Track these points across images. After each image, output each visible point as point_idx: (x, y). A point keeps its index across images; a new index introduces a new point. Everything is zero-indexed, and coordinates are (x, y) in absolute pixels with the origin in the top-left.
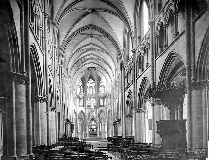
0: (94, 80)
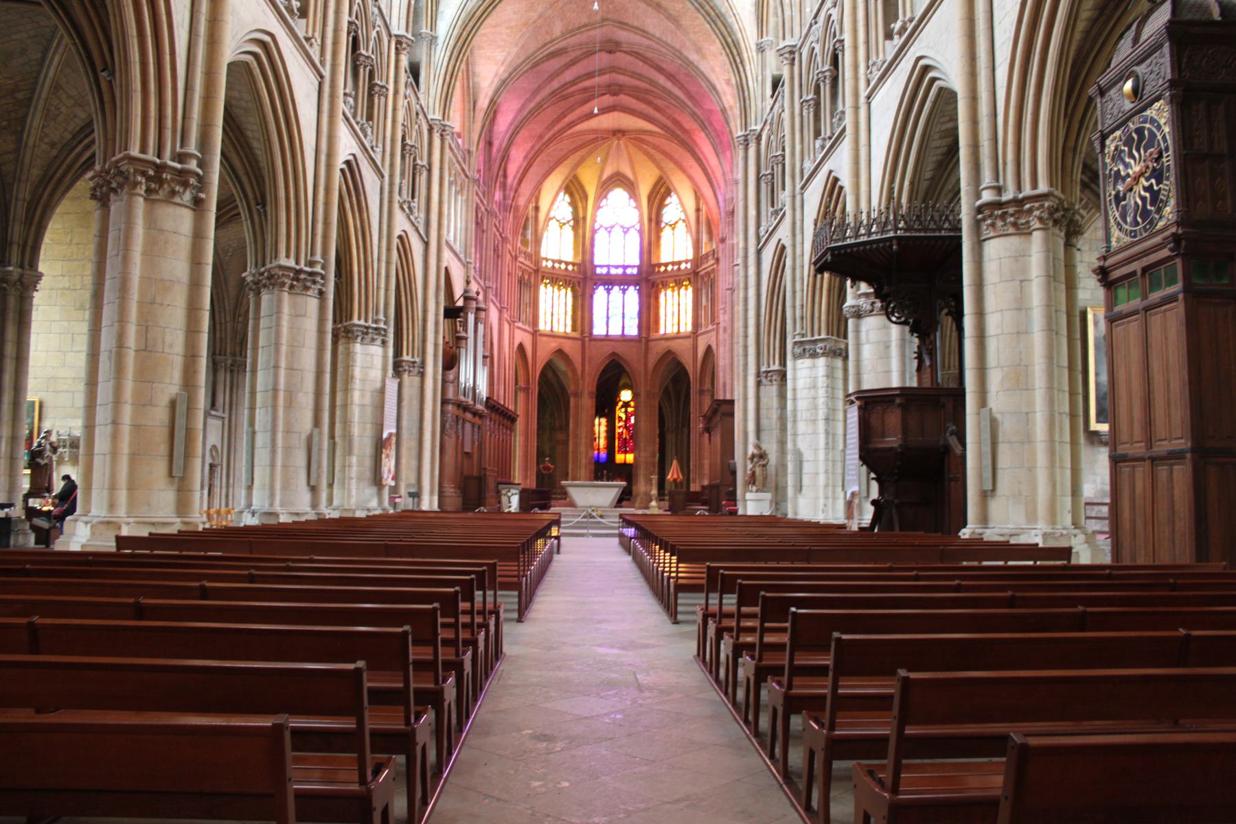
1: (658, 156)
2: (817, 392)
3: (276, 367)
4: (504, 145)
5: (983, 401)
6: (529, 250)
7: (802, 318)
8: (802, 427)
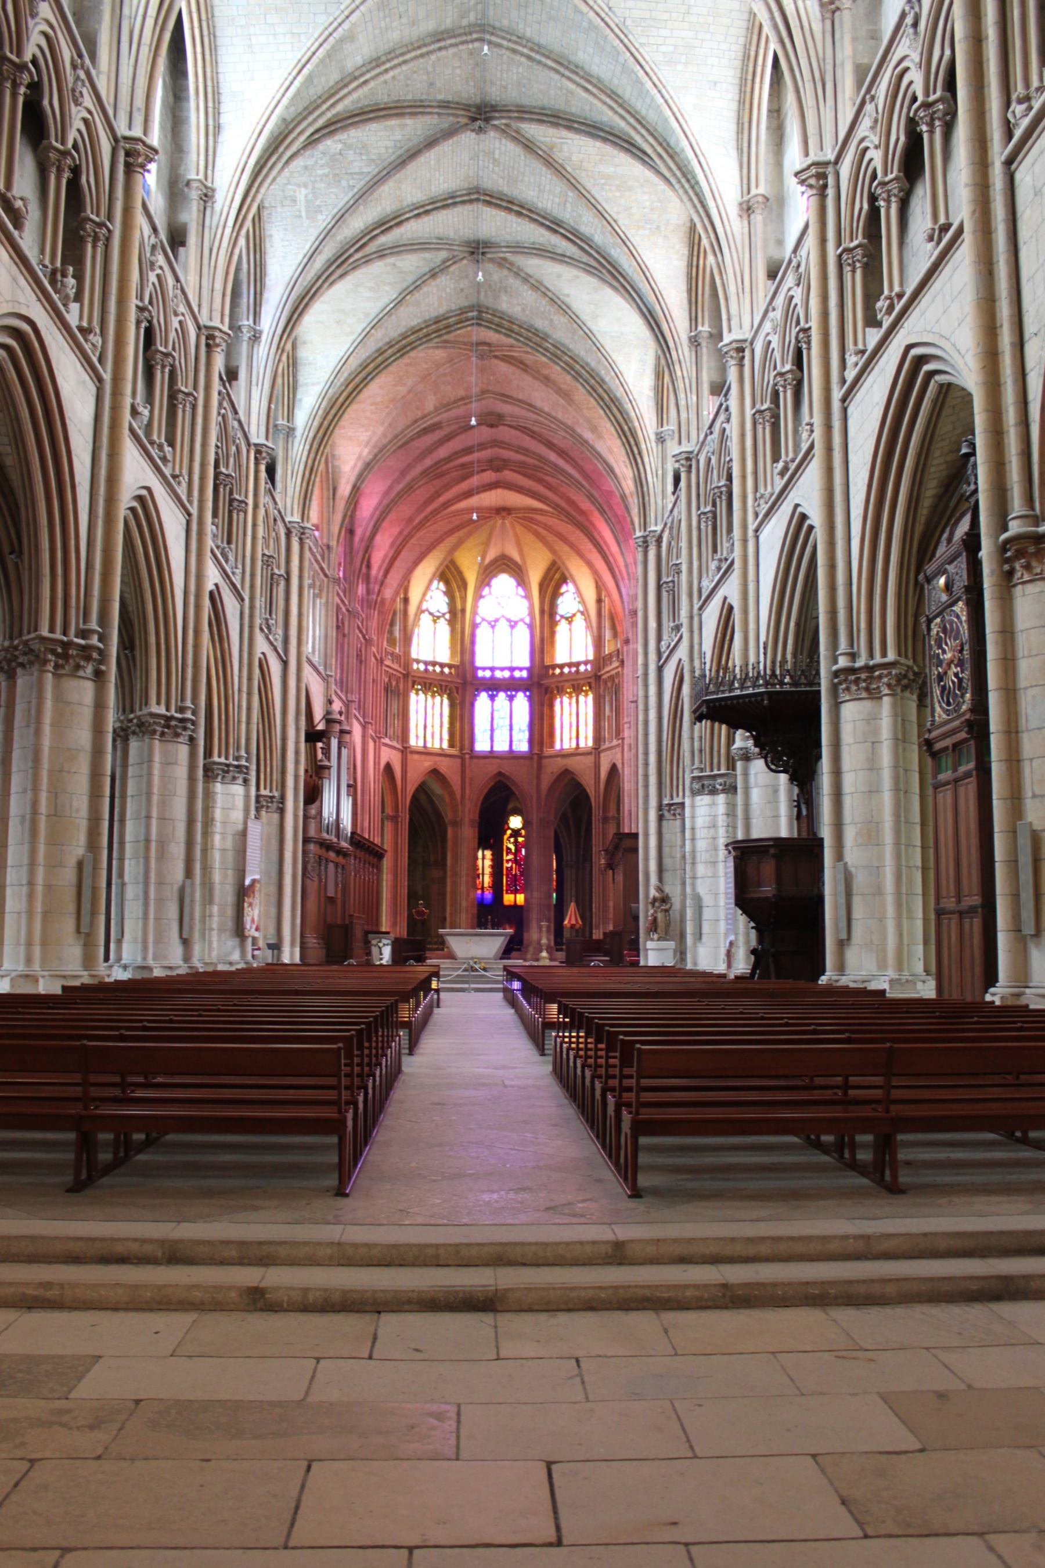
0: (522, 580)
1: (551, 538)
2: (716, 832)
3: (148, 817)
4: (368, 534)
5: (839, 856)
6: (397, 651)
7: (701, 751)
8: (701, 869)
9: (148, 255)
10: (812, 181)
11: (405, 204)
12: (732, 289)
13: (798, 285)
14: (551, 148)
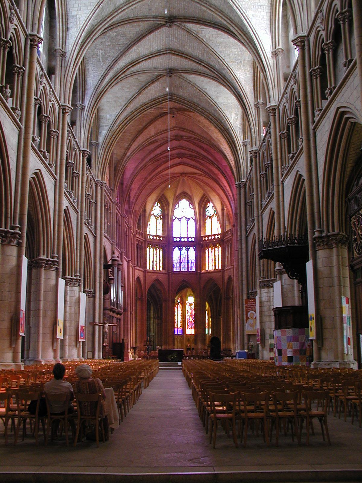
0: (191, 201)
1: (202, 184)
9: (39, 79)
10: (299, 44)
11: (141, 55)
12: (270, 85)
13: (295, 84)
14: (198, 33)
